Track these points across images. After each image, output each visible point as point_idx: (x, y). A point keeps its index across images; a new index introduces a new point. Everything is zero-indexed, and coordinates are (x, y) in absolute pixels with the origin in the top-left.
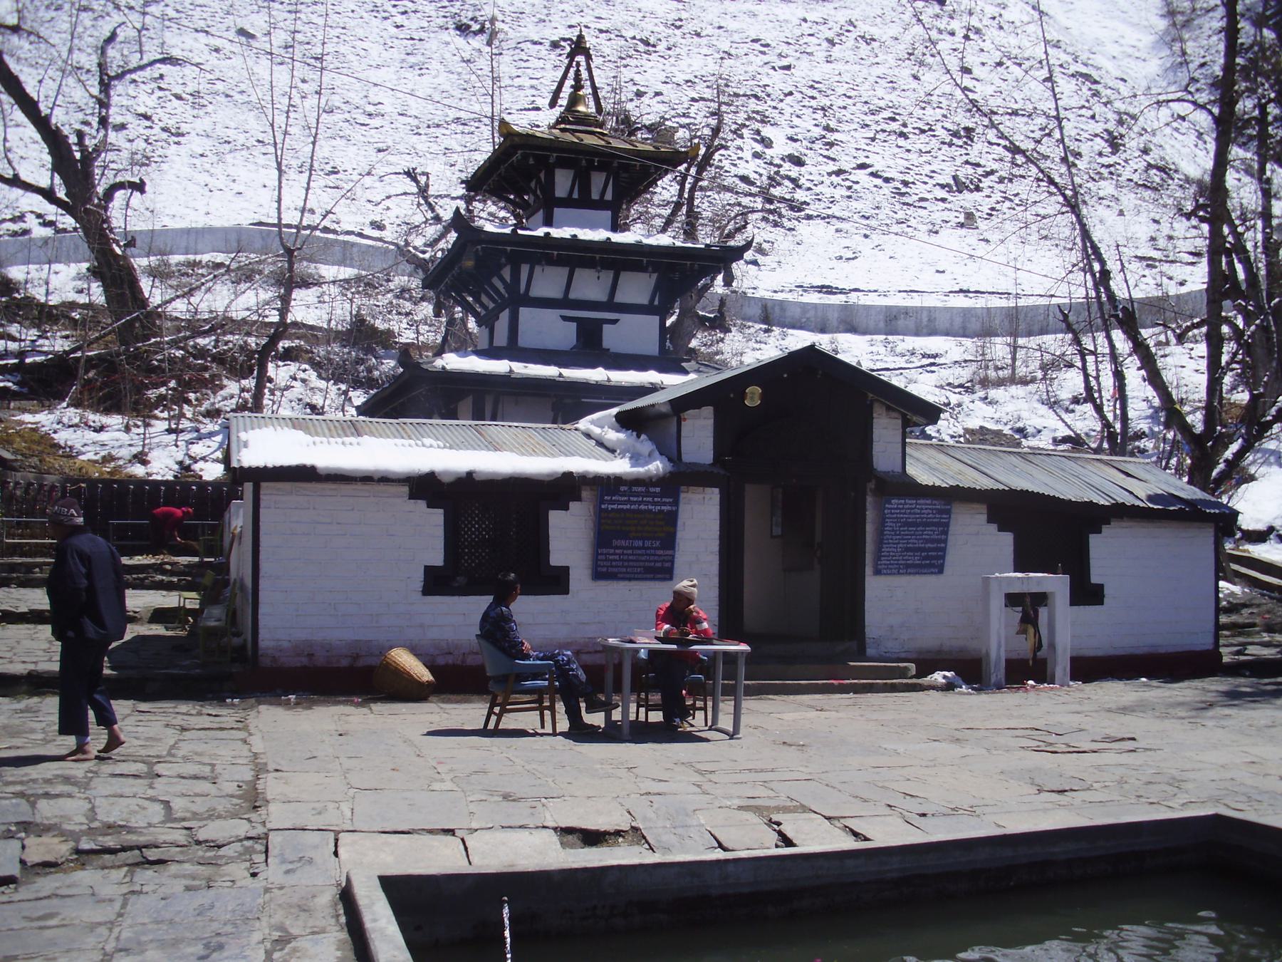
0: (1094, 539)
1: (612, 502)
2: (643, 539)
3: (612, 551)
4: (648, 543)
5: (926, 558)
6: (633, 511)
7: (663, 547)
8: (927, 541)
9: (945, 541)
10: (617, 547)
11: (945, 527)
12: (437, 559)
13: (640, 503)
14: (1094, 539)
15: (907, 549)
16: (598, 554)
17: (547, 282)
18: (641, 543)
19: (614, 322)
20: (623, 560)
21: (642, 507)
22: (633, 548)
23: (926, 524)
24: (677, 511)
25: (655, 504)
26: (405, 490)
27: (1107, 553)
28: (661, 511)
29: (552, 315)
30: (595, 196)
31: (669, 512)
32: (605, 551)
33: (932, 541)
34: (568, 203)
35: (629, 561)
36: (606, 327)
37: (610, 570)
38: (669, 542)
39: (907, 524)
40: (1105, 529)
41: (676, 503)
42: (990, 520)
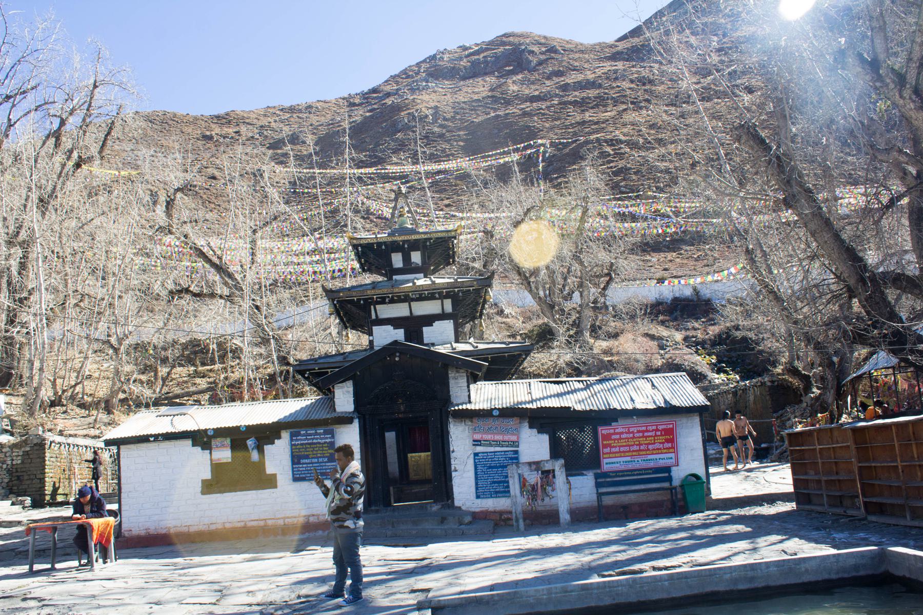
1: (297, 440)
2: (317, 458)
4: (321, 460)
6: (310, 444)
12: (208, 475)
13: (313, 439)
26: (189, 442)
28: (325, 443)
41: (333, 437)
42: (531, 427)
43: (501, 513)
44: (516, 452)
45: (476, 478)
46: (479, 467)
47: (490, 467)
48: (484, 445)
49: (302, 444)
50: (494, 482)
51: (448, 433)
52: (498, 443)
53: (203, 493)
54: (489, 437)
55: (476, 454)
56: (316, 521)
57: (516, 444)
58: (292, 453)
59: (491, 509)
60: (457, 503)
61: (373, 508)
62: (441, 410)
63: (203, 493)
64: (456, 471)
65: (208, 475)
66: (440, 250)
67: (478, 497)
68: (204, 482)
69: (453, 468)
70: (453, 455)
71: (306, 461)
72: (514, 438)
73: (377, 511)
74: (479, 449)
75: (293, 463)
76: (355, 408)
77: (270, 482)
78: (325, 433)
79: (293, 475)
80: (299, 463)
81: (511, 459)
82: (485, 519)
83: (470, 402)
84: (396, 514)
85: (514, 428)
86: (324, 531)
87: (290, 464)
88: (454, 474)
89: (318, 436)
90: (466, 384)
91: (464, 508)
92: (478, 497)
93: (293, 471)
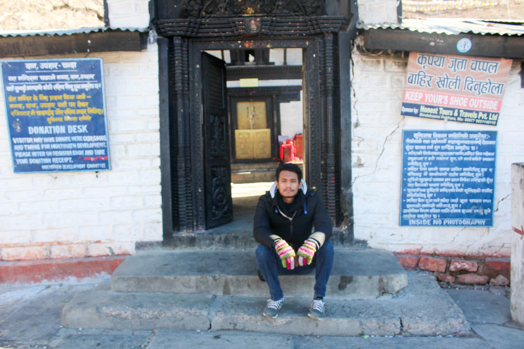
2: (65, 124)
3: (29, 140)
4: (72, 129)
6: (48, 93)
10: (34, 136)
16: (13, 144)
18: (62, 129)
20: (45, 150)
21: (58, 87)
22: (54, 135)
24: (101, 89)
25: (73, 82)
28: (81, 91)
31: (92, 90)
32: (21, 140)
35: (52, 150)
37: (32, 161)
38: (97, 126)
41: (98, 78)
43: (449, 258)
44: (493, 135)
45: (404, 184)
46: (413, 162)
47: (436, 163)
48: (427, 117)
49: (30, 93)
50: (440, 195)
51: (349, 84)
52: (457, 115)
54: (438, 99)
55: (408, 134)
56: (67, 254)
57: (490, 117)
58: (9, 111)
59: (428, 249)
60: (358, 234)
61: (184, 234)
62: (335, 35)
64: (360, 165)
67: (404, 223)
69: (354, 160)
70: (355, 133)
71: (41, 130)
72: (490, 105)
73: (192, 241)
74: (412, 123)
75: (13, 134)
76: (153, 21)
78: (82, 68)
79: (15, 158)
80: (25, 134)
81: (482, 148)
82: (416, 267)
83: (400, 21)
84: (232, 249)
85: (495, 82)
86: (79, 275)
88: (355, 172)
91: (372, 243)
92: (404, 223)
93: (14, 151)
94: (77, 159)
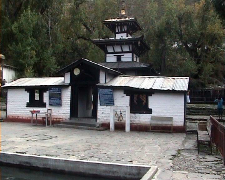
0: (150, 98)
1: (51, 91)
5: (109, 102)
7: (59, 100)
8: (109, 98)
9: (113, 98)
11: (112, 95)
12: (28, 101)
14: (150, 98)
15: (105, 100)
17: (110, 50)
18: (55, 99)
19: (123, 55)
23: (108, 94)
27: (153, 102)
29: (112, 55)
30: (123, 31)
31: (60, 93)
33: (110, 98)
34: (119, 33)
36: (122, 56)
39: (104, 95)
40: (153, 95)
41: (60, 91)
42: (124, 93)
53: (27, 107)
63: (27, 107)
65: (28, 101)
66: (132, 27)
68: (27, 103)
71: (53, 99)
77: (44, 105)
87: (48, 99)
89: (56, 91)
90: (105, 76)
94: (57, 104)
